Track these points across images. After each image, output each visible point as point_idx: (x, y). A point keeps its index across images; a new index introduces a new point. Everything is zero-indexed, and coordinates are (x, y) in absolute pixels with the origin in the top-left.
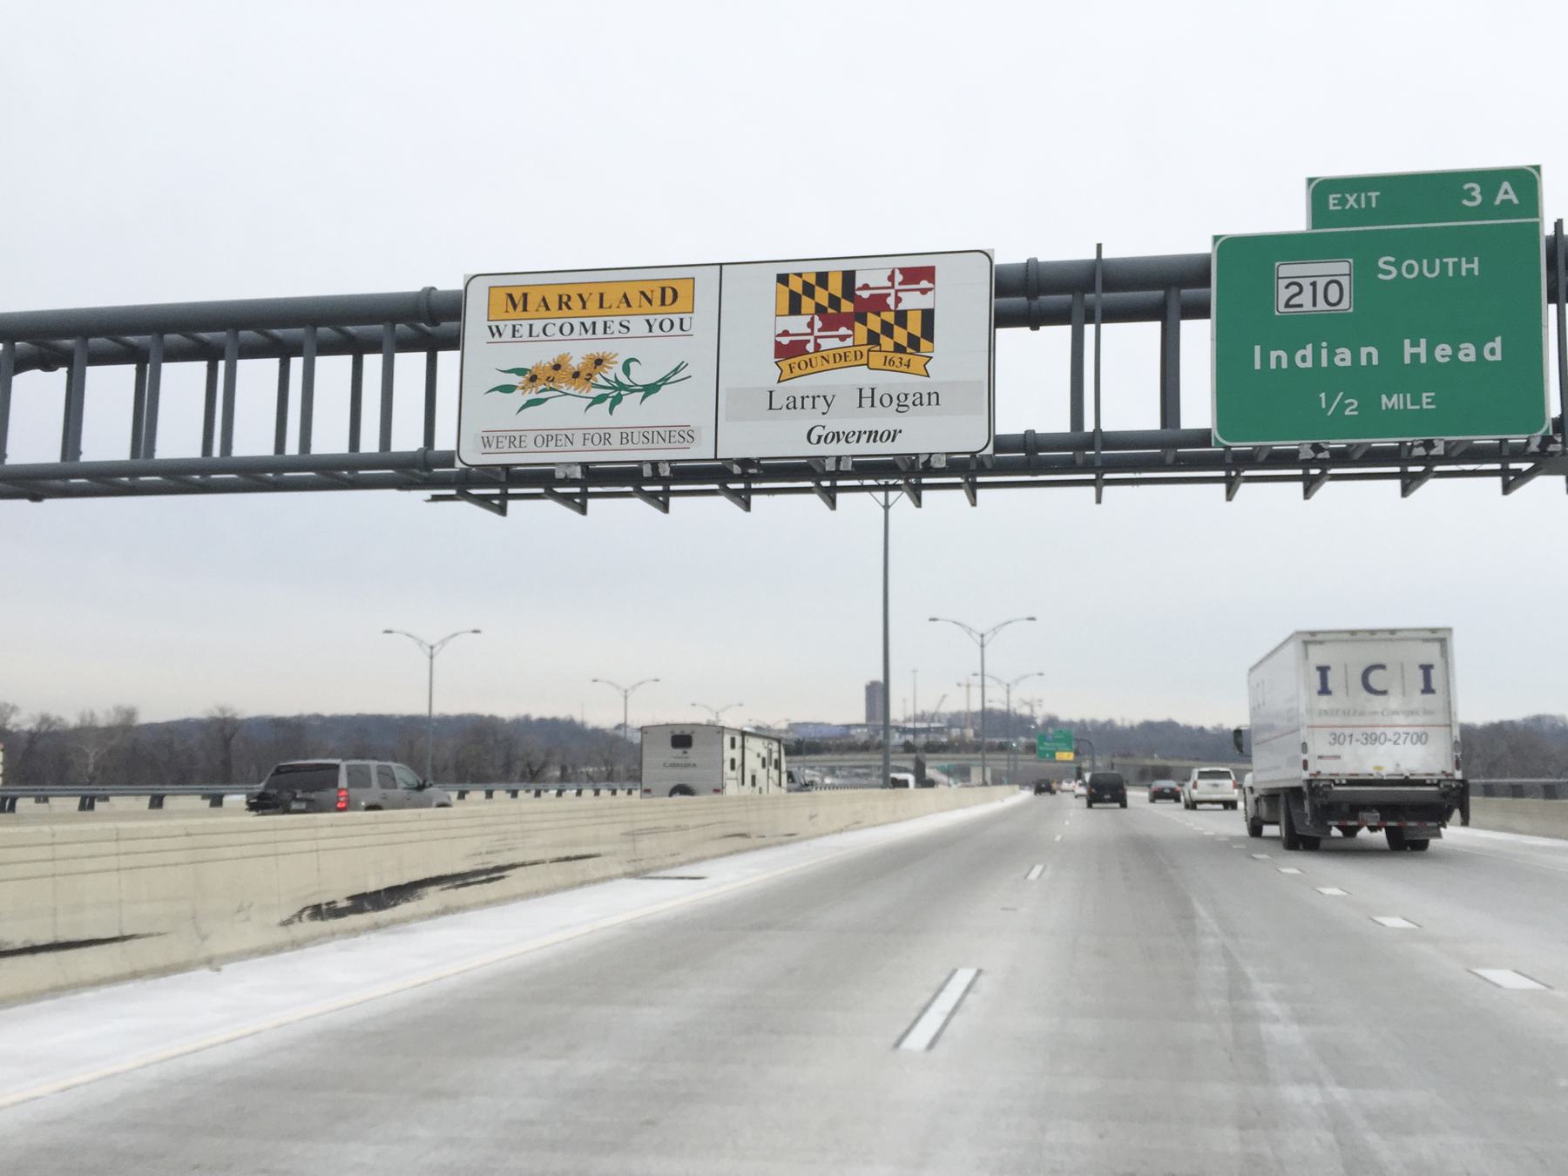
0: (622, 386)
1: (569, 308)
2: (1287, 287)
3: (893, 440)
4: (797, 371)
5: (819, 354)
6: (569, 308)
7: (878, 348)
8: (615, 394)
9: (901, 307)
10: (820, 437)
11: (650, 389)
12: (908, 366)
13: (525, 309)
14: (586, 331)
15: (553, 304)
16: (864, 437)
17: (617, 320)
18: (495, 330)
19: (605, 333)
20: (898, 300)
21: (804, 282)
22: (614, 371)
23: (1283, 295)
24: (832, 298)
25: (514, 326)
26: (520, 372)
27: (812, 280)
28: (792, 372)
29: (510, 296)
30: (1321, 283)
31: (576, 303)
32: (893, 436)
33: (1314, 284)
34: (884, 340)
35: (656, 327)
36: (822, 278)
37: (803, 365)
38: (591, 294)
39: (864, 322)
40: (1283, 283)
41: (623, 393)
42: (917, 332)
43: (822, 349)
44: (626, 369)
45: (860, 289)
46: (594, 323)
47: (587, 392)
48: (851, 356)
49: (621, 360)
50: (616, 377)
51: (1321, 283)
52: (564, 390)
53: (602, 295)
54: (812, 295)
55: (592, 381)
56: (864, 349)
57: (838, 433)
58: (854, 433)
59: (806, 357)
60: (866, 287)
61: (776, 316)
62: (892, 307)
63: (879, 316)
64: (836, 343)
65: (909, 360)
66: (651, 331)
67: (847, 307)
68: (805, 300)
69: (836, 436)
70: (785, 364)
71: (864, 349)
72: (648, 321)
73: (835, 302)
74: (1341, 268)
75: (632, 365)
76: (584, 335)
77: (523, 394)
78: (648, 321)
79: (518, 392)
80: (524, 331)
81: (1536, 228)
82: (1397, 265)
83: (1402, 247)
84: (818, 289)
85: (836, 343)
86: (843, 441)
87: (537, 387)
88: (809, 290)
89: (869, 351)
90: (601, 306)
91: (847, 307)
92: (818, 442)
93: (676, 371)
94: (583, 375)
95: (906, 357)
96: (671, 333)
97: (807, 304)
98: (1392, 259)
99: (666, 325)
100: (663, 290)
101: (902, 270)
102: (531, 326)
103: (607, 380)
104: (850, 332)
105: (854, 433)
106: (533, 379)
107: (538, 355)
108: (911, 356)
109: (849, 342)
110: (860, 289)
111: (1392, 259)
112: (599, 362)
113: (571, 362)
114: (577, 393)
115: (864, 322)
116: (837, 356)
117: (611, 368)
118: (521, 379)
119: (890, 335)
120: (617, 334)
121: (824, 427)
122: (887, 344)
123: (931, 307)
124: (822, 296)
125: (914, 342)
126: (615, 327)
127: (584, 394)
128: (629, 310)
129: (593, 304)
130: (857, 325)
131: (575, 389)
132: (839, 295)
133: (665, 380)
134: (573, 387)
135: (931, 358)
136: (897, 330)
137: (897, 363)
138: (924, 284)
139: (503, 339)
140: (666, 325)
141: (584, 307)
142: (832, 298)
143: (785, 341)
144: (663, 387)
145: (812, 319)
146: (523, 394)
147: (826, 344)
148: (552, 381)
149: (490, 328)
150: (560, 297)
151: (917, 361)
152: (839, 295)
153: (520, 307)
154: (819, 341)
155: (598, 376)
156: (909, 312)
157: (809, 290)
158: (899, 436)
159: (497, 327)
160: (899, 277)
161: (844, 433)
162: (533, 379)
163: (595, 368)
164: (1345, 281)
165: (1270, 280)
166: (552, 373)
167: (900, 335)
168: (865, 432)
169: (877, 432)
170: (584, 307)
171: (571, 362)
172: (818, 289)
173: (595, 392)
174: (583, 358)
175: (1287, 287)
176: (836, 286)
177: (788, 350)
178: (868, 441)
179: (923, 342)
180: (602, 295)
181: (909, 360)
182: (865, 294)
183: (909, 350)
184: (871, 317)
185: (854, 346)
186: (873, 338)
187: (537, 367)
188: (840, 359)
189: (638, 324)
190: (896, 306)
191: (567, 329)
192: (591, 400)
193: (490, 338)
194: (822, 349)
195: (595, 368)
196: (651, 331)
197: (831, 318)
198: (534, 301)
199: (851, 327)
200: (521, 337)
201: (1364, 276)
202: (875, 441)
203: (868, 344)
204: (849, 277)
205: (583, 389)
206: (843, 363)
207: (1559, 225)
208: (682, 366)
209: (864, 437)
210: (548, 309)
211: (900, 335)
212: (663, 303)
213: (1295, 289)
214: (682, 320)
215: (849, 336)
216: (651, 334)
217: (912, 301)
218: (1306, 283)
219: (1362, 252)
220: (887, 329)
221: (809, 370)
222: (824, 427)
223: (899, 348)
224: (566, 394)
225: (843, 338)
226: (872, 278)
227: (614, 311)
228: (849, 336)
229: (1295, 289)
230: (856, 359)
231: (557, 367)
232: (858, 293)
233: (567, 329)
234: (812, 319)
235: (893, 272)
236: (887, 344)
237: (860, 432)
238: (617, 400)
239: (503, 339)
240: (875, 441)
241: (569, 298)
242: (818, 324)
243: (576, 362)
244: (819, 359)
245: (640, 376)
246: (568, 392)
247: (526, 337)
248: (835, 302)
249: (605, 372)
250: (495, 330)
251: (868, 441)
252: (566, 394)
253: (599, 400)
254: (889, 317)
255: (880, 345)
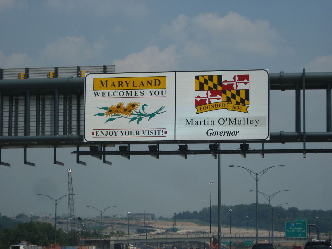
0: (141, 114)
1: (122, 86)
3: (236, 135)
5: (210, 105)
6: (122, 86)
7: (230, 103)
8: (139, 117)
9: (238, 89)
10: (211, 133)
11: (152, 116)
12: (241, 109)
13: (107, 86)
14: (129, 95)
15: (117, 85)
16: (226, 134)
17: (139, 91)
18: (96, 94)
19: (135, 95)
20: (237, 86)
21: (204, 79)
22: (139, 109)
25: (103, 92)
26: (105, 109)
27: (207, 78)
28: (201, 110)
29: (101, 81)
31: (124, 84)
32: (236, 133)
34: (232, 100)
37: (205, 108)
38: (130, 81)
39: (225, 94)
41: (142, 117)
42: (244, 97)
44: (143, 108)
45: (224, 82)
46: (131, 92)
47: (130, 116)
48: (221, 105)
49: (141, 105)
50: (139, 111)
52: (121, 115)
53: (134, 82)
55: (131, 112)
56: (226, 103)
57: (217, 132)
58: (223, 132)
59: (206, 105)
60: (226, 81)
61: (195, 91)
62: (235, 88)
63: (230, 91)
64: (216, 101)
65: (241, 107)
67: (219, 88)
69: (217, 133)
70: (199, 107)
71: (226, 103)
72: (150, 91)
73: (215, 86)
75: (145, 107)
76: (128, 96)
77: (107, 116)
78: (150, 91)
79: (105, 116)
80: (106, 94)
84: (209, 82)
85: (216, 101)
86: (219, 135)
88: (206, 82)
89: (227, 103)
90: (134, 86)
91: (219, 88)
92: (210, 135)
93: (161, 109)
94: (128, 110)
95: (240, 106)
96: (159, 96)
97: (206, 87)
99: (157, 93)
100: (155, 80)
101: (238, 76)
102: (109, 92)
103: (137, 112)
104: (221, 97)
105: (223, 132)
106: (110, 111)
107: (112, 102)
108: (241, 106)
109: (220, 100)
110: (224, 82)
113: (123, 105)
114: (126, 116)
115: (225, 94)
116: (216, 105)
117: (138, 108)
118: (106, 111)
119: (234, 98)
121: (212, 130)
122: (233, 101)
123: (248, 89)
125: (242, 101)
126: (139, 93)
127: (128, 117)
128: (143, 88)
129: (131, 84)
130: (223, 95)
131: (125, 115)
133: (157, 112)
134: (124, 114)
135: (249, 107)
136: (237, 97)
137: (237, 108)
138: (246, 81)
139: (99, 97)
140: (157, 93)
141: (128, 86)
143: (198, 99)
145: (208, 92)
146: (107, 116)
147: (212, 101)
148: (117, 112)
149: (94, 93)
150: (119, 82)
153: (105, 85)
155: (133, 111)
156: (241, 91)
158: (238, 133)
159: (97, 93)
160: (237, 78)
161: (219, 132)
162: (110, 111)
163: (132, 108)
166: (117, 109)
169: (230, 132)
170: (128, 86)
171: (123, 105)
172: (209, 82)
173: (132, 116)
174: (128, 104)
176: (215, 81)
177: (200, 103)
178: (227, 135)
179: (246, 101)
180: (134, 82)
181: (241, 107)
182: (226, 84)
183: (241, 104)
184: (228, 92)
185: (222, 102)
186: (229, 99)
187: (111, 107)
188: (217, 106)
189: (147, 92)
190: (236, 88)
191: (122, 94)
192: (131, 119)
193: (95, 97)
195: (132, 108)
197: (214, 92)
198: (110, 84)
199: (221, 95)
200: (105, 96)
202: (230, 135)
203: (227, 101)
204: (220, 77)
205: (128, 115)
206: (218, 108)
208: (163, 108)
209: (226, 134)
210: (115, 86)
212: (155, 85)
215: (220, 98)
217: (242, 87)
221: (207, 110)
222: (212, 130)
223: (237, 103)
225: (218, 99)
227: (138, 88)
228: (220, 98)
230: (223, 106)
231: (118, 107)
232: (223, 83)
233: (122, 94)
234: (208, 92)
235: (235, 76)
236: (233, 101)
238: (140, 119)
239: (99, 97)
240: (230, 135)
241: (122, 83)
242: (210, 94)
243: (125, 106)
244: (210, 106)
245: (148, 111)
246: (123, 116)
247: (107, 97)
248: (215, 86)
249: (136, 109)
250: (96, 94)
251: (227, 135)
252: (122, 117)
253: (133, 119)
254: (234, 92)
255: (231, 102)
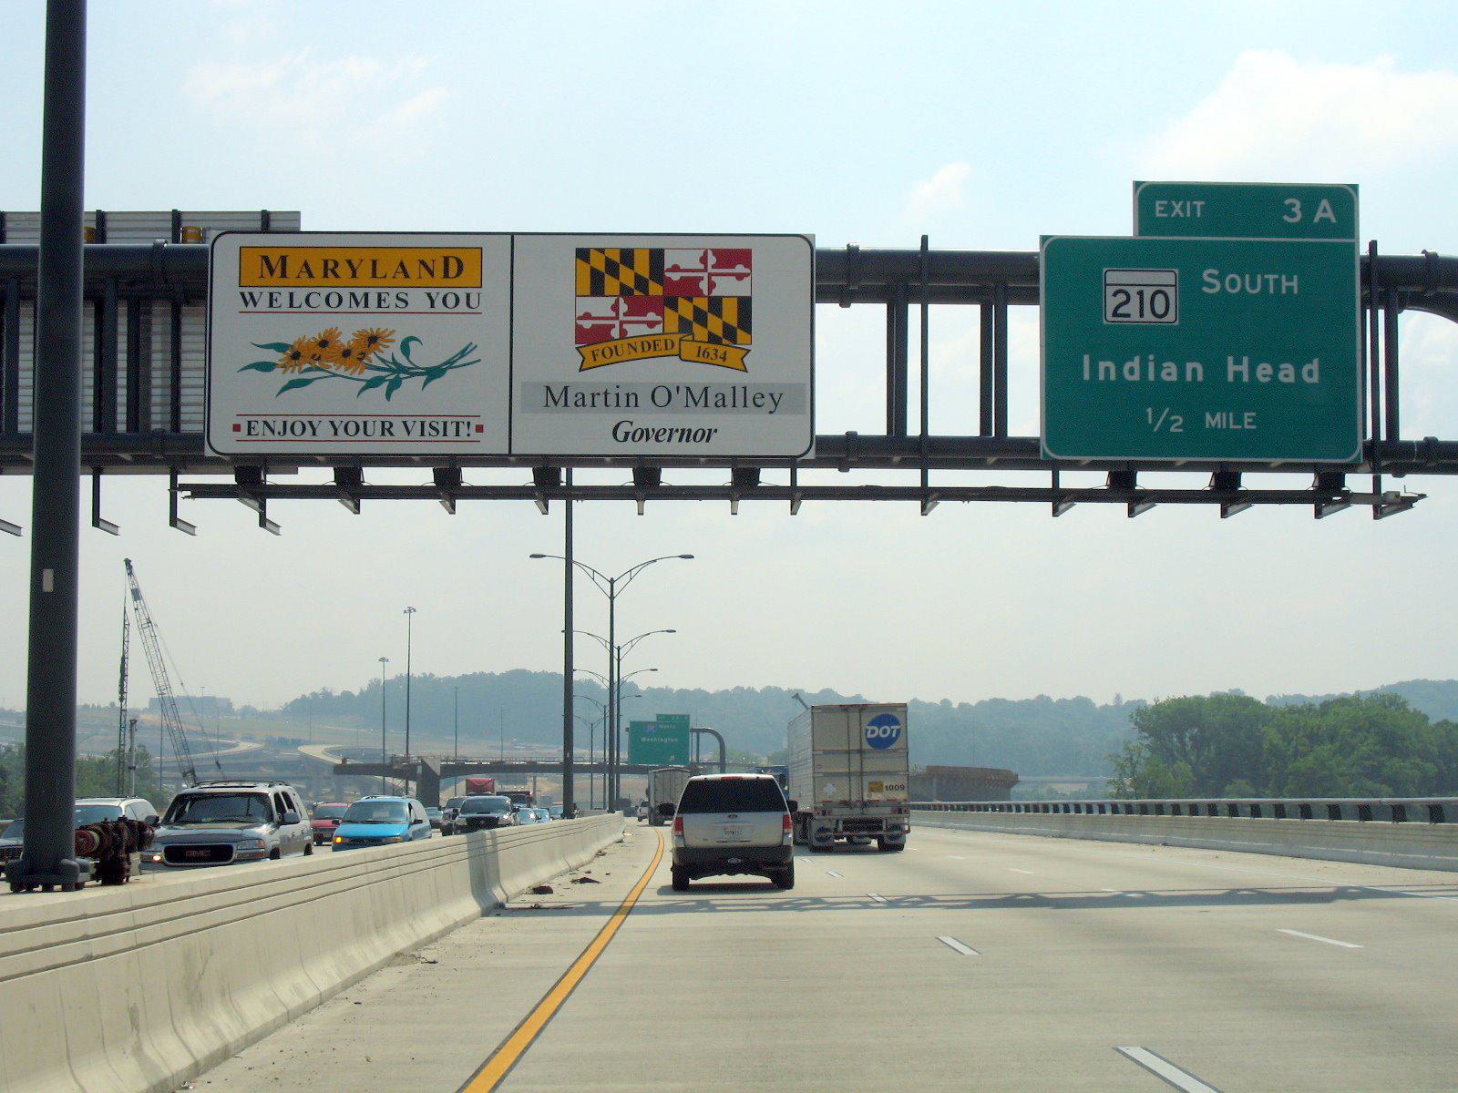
0: (401, 369)
2: (1115, 295)
3: (707, 441)
4: (600, 359)
7: (690, 338)
8: (392, 377)
9: (715, 293)
10: (627, 434)
11: (433, 373)
12: (724, 359)
16: (676, 436)
20: (712, 285)
22: (392, 351)
23: (1112, 303)
24: (638, 279)
26: (279, 347)
28: (595, 360)
30: (1148, 293)
32: (707, 435)
33: (1141, 294)
35: (438, 302)
36: (627, 256)
37: (607, 353)
39: (674, 307)
40: (1110, 290)
41: (402, 375)
43: (628, 336)
44: (405, 348)
45: (669, 270)
48: (662, 345)
50: (393, 359)
51: (1148, 293)
52: (333, 370)
54: (616, 275)
56: (676, 338)
57: (647, 430)
58: (665, 430)
59: (612, 344)
60: (676, 269)
62: (705, 293)
64: (644, 330)
66: (432, 306)
67: (655, 289)
68: (608, 279)
69: (645, 434)
70: (587, 351)
71: (676, 338)
74: (1167, 278)
75: (412, 345)
76: (355, 308)
81: (1353, 247)
82: (1221, 278)
83: (1228, 260)
85: (644, 330)
87: (300, 365)
88: (612, 268)
89: (680, 340)
91: (655, 289)
92: (626, 439)
93: (463, 353)
94: (355, 354)
95: (721, 349)
96: (456, 310)
97: (611, 284)
98: (1216, 272)
99: (451, 301)
103: (383, 361)
104: (659, 318)
105: (665, 430)
106: (296, 356)
107: (303, 328)
109: (658, 329)
110: (669, 270)
111: (1216, 272)
112: (373, 339)
115: (674, 307)
117: (388, 347)
118: (281, 356)
119: (704, 323)
120: (393, 309)
121: (632, 423)
123: (746, 294)
124: (627, 276)
127: (356, 375)
130: (668, 311)
132: (646, 275)
133: (450, 364)
134: (343, 367)
135: (749, 351)
136: (711, 318)
137: (712, 356)
138: (740, 269)
139: (258, 308)
140: (451, 301)
142: (638, 279)
144: (449, 371)
145: (617, 301)
147: (633, 330)
151: (733, 354)
152: (646, 275)
154: (625, 326)
155: (372, 356)
157: (612, 268)
158: (714, 436)
160: (712, 260)
161: (653, 430)
162: (296, 356)
163: (369, 346)
164: (1171, 292)
165: (1100, 284)
166: (318, 351)
167: (715, 325)
168: (677, 430)
173: (369, 374)
174: (354, 334)
175: (1115, 295)
176: (643, 267)
177: (591, 337)
178: (680, 440)
181: (725, 353)
182: (675, 277)
183: (725, 341)
184: (682, 302)
186: (685, 326)
188: (650, 348)
190: (710, 292)
194: (628, 336)
195: (369, 346)
196: (432, 306)
197: (637, 299)
199: (662, 314)
200: (280, 307)
201: (1189, 287)
202: (688, 440)
204: (657, 256)
205: (355, 371)
206: (651, 353)
207: (1373, 245)
208: (470, 348)
209: (676, 436)
211: (715, 325)
213: (1122, 298)
214: (468, 296)
215: (658, 323)
216: (432, 310)
217: (727, 287)
218: (1133, 291)
219: (1188, 263)
220: (700, 317)
223: (713, 339)
224: (335, 375)
225: (651, 324)
226: (681, 260)
228: (658, 323)
229: (1122, 298)
230: (666, 349)
231: (323, 343)
232: (667, 274)
234: (617, 301)
235: (706, 254)
237: (671, 430)
239: (258, 308)
240: (688, 440)
242: (623, 307)
243: (346, 339)
245: (423, 357)
247: (285, 307)
248: (641, 282)
249: (381, 351)
251: (680, 440)
254: (702, 304)
255: (693, 334)
